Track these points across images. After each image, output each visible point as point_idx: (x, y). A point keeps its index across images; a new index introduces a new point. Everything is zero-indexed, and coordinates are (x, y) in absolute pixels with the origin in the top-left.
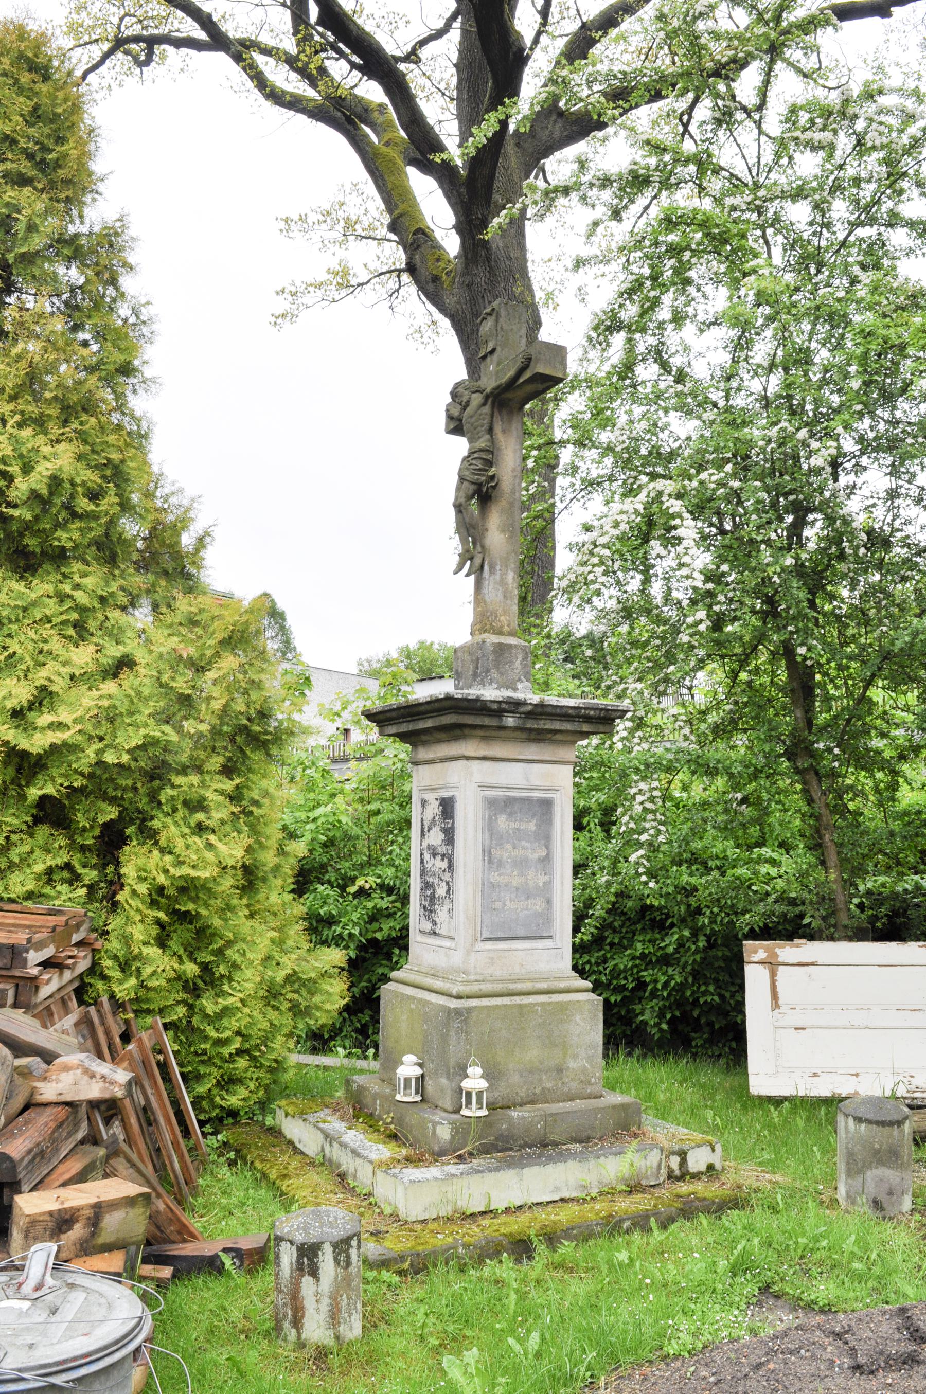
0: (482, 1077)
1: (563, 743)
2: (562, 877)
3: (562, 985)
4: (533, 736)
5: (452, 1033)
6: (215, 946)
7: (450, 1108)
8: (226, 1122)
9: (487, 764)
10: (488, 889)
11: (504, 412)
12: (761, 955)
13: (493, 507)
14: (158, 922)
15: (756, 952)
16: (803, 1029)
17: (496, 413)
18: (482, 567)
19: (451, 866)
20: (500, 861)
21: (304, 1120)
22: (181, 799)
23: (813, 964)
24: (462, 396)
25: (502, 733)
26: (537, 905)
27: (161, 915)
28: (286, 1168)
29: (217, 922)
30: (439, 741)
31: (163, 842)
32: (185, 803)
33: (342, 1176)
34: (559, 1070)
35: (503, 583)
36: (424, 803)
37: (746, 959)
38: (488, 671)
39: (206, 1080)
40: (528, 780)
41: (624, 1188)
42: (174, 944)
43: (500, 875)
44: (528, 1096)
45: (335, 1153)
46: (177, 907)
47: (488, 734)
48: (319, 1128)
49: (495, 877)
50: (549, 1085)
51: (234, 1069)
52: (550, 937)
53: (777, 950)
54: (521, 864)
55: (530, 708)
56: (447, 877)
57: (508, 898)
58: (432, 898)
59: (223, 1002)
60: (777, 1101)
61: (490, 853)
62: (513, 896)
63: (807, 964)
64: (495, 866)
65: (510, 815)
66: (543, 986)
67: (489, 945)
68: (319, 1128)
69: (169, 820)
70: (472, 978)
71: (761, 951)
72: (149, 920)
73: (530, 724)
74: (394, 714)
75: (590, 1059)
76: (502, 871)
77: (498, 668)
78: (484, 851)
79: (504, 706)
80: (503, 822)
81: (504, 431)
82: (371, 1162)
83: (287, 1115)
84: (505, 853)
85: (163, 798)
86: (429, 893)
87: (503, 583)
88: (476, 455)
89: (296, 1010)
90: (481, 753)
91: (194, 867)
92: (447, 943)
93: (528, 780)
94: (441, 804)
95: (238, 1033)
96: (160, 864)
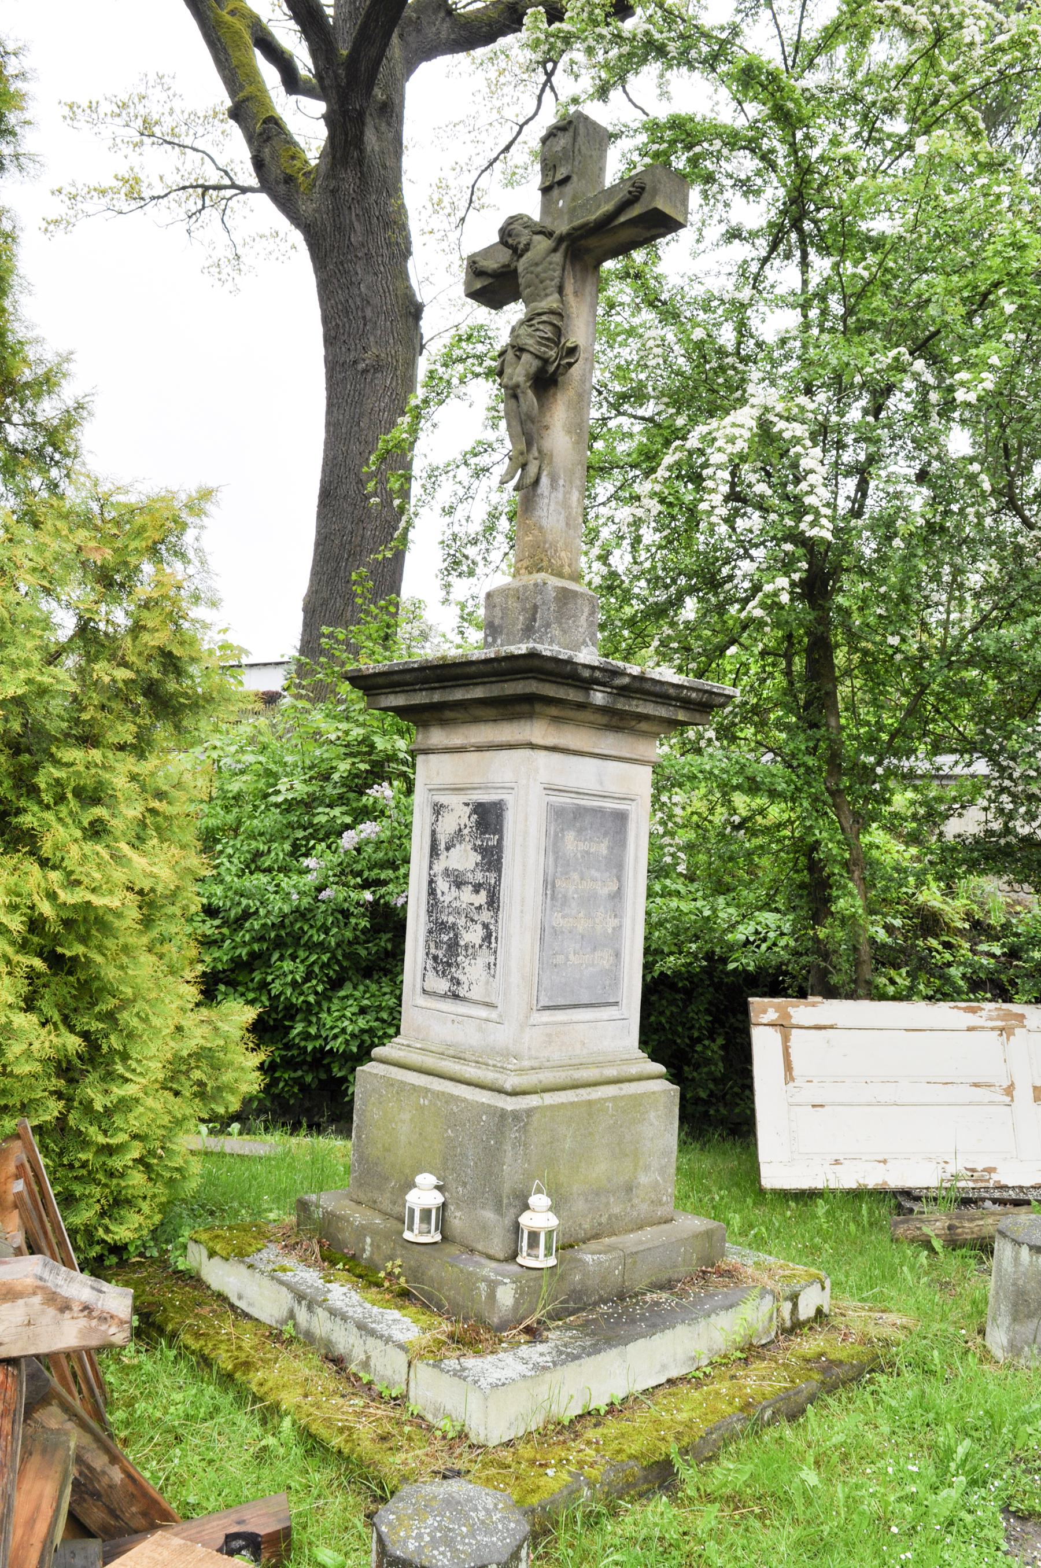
0: (550, 1209)
1: (644, 734)
2: (634, 920)
3: (634, 1070)
4: (615, 721)
5: (508, 1147)
6: (103, 1007)
7: (501, 1255)
8: (107, 1263)
9: (557, 757)
10: (546, 935)
11: (578, 267)
12: (771, 1015)
13: (559, 396)
14: (32, 976)
15: (765, 1012)
16: (822, 1106)
17: (568, 267)
18: (537, 482)
19: (493, 902)
20: (565, 897)
21: (250, 1266)
22: (73, 784)
23: (831, 1027)
24: (518, 235)
25: (581, 715)
26: (604, 959)
27: (38, 964)
28: (240, 1348)
29: (110, 973)
30: (476, 720)
31: (47, 849)
32: (78, 792)
33: (338, 1362)
34: (629, 1189)
35: (565, 504)
36: (438, 809)
37: (753, 1020)
38: (548, 625)
39: (83, 1205)
40: (601, 784)
41: (739, 1354)
42: (47, 1005)
43: (563, 917)
44: (592, 1227)
45: (321, 1324)
46: (59, 950)
47: (562, 714)
48: (282, 1283)
49: (557, 920)
50: (616, 1210)
51: (127, 1187)
52: (616, 1004)
53: (790, 1009)
54: (589, 900)
55: (626, 680)
56: (486, 916)
57: (571, 950)
58: (453, 946)
59: (119, 1091)
60: (806, 1197)
61: (554, 886)
62: (578, 946)
63: (824, 1028)
64: (558, 904)
65: (580, 831)
66: (611, 1072)
67: (547, 1017)
68: (282, 1283)
69: (49, 816)
70: (526, 1063)
71: (771, 1010)
72: (19, 972)
73: (622, 705)
74: (408, 677)
75: (662, 1170)
76: (567, 911)
77: (560, 623)
78: (545, 881)
79: (597, 674)
80: (571, 842)
81: (576, 293)
82: (401, 1347)
83: (212, 1254)
84: (568, 887)
85: (41, 780)
86: (445, 938)
87: (565, 504)
88: (544, 318)
89: (202, 1093)
90: (550, 741)
91: (93, 890)
92: (483, 1013)
93: (601, 784)
94: (475, 811)
95: (135, 1137)
96: (43, 885)
